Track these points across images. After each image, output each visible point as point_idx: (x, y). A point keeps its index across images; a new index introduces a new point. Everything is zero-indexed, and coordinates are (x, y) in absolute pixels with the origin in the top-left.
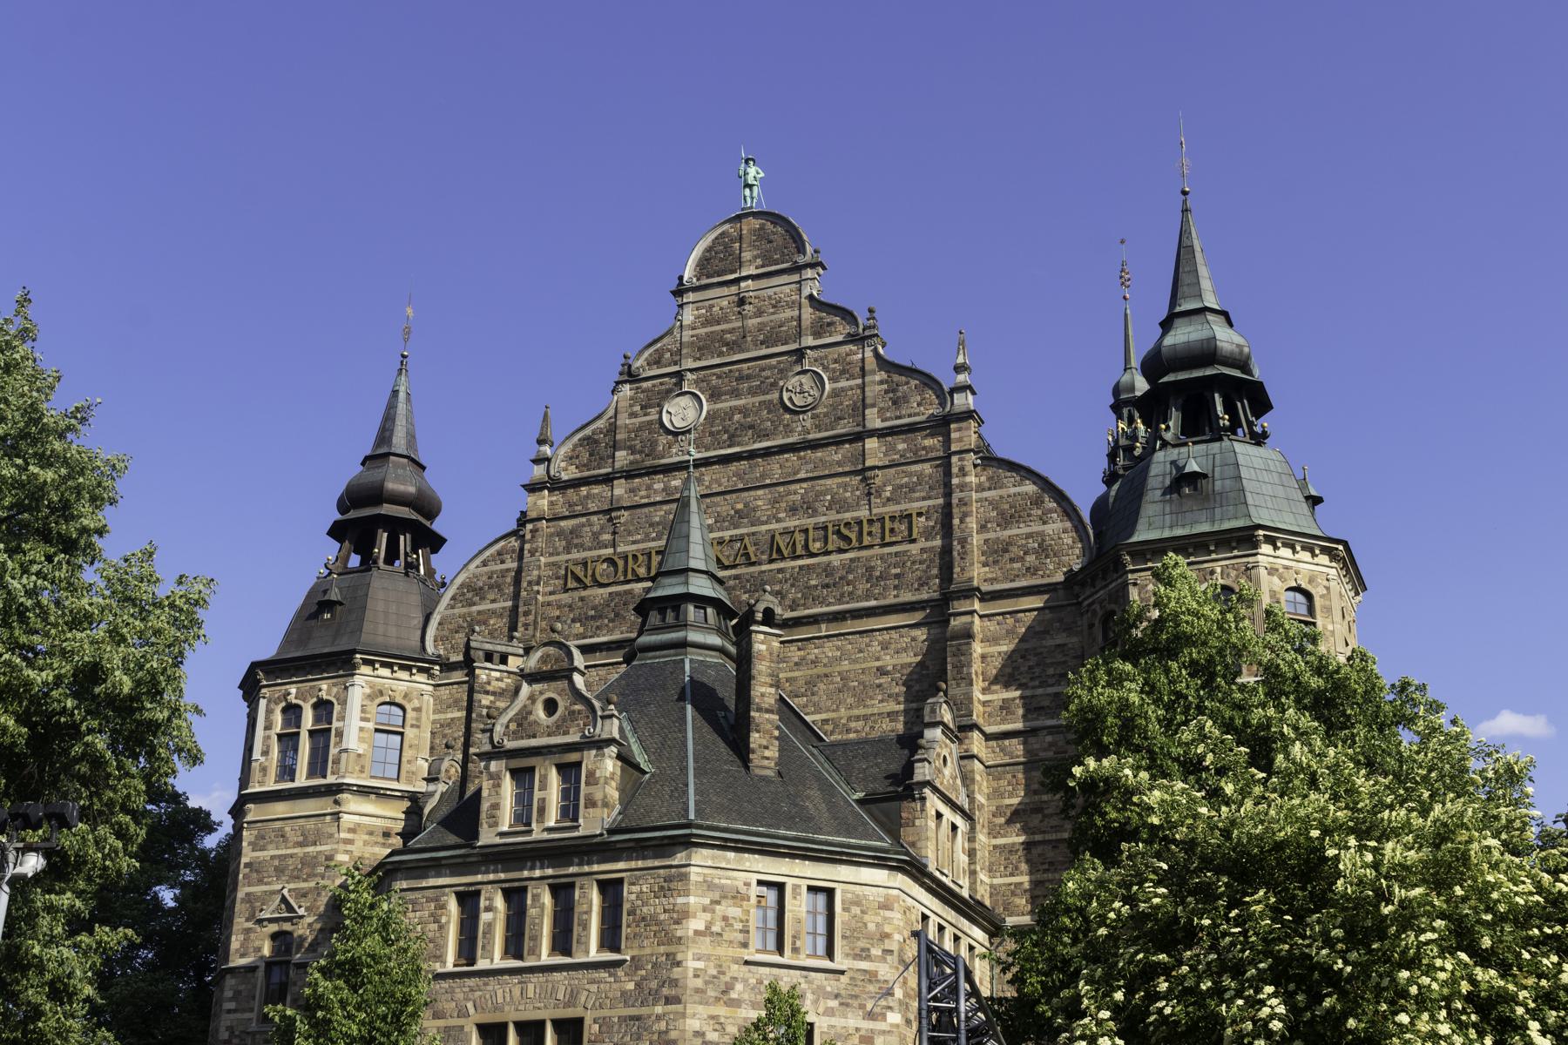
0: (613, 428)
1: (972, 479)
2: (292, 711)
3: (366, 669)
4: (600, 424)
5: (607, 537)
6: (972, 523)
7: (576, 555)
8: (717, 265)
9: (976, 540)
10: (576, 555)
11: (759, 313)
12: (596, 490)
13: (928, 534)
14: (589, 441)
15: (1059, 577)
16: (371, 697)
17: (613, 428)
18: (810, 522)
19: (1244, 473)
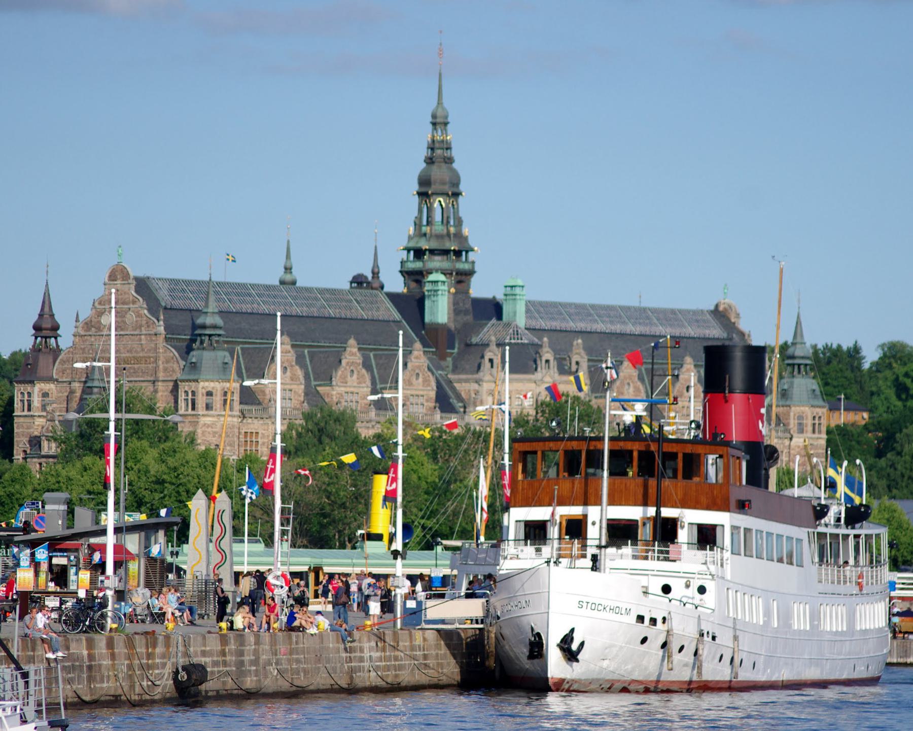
0: (91, 321)
1: (161, 351)
2: (22, 393)
3: (38, 385)
4: (89, 319)
5: (91, 352)
6: (160, 362)
7: (85, 355)
8: (112, 278)
9: (161, 367)
10: (85, 355)
11: (121, 294)
12: (89, 338)
13: (153, 363)
14: (86, 323)
15: (175, 379)
16: (40, 392)
17: (91, 321)
18: (130, 355)
19: (203, 362)
